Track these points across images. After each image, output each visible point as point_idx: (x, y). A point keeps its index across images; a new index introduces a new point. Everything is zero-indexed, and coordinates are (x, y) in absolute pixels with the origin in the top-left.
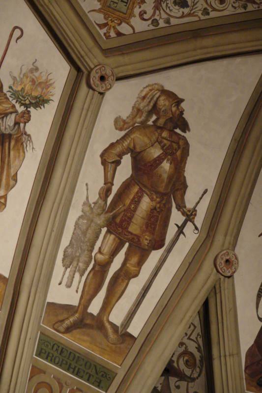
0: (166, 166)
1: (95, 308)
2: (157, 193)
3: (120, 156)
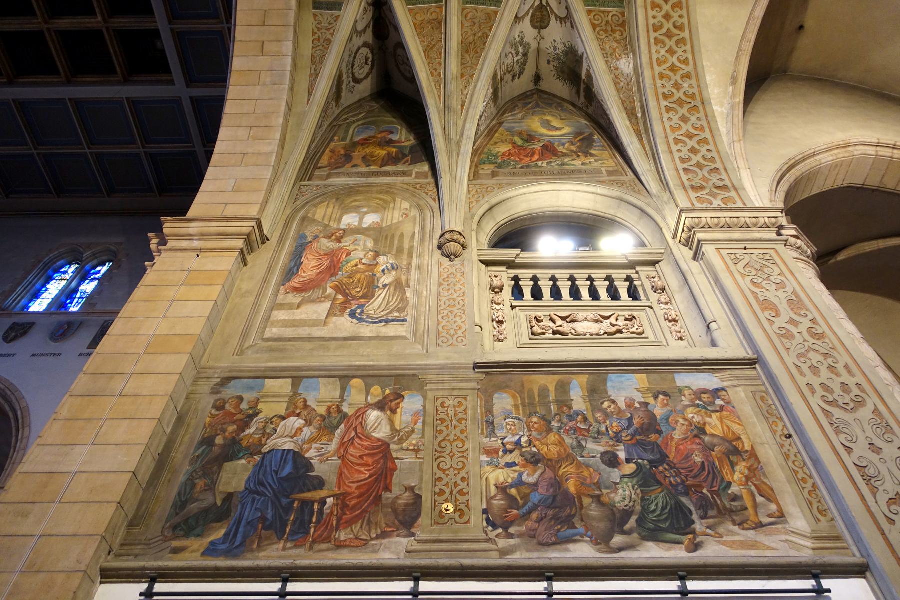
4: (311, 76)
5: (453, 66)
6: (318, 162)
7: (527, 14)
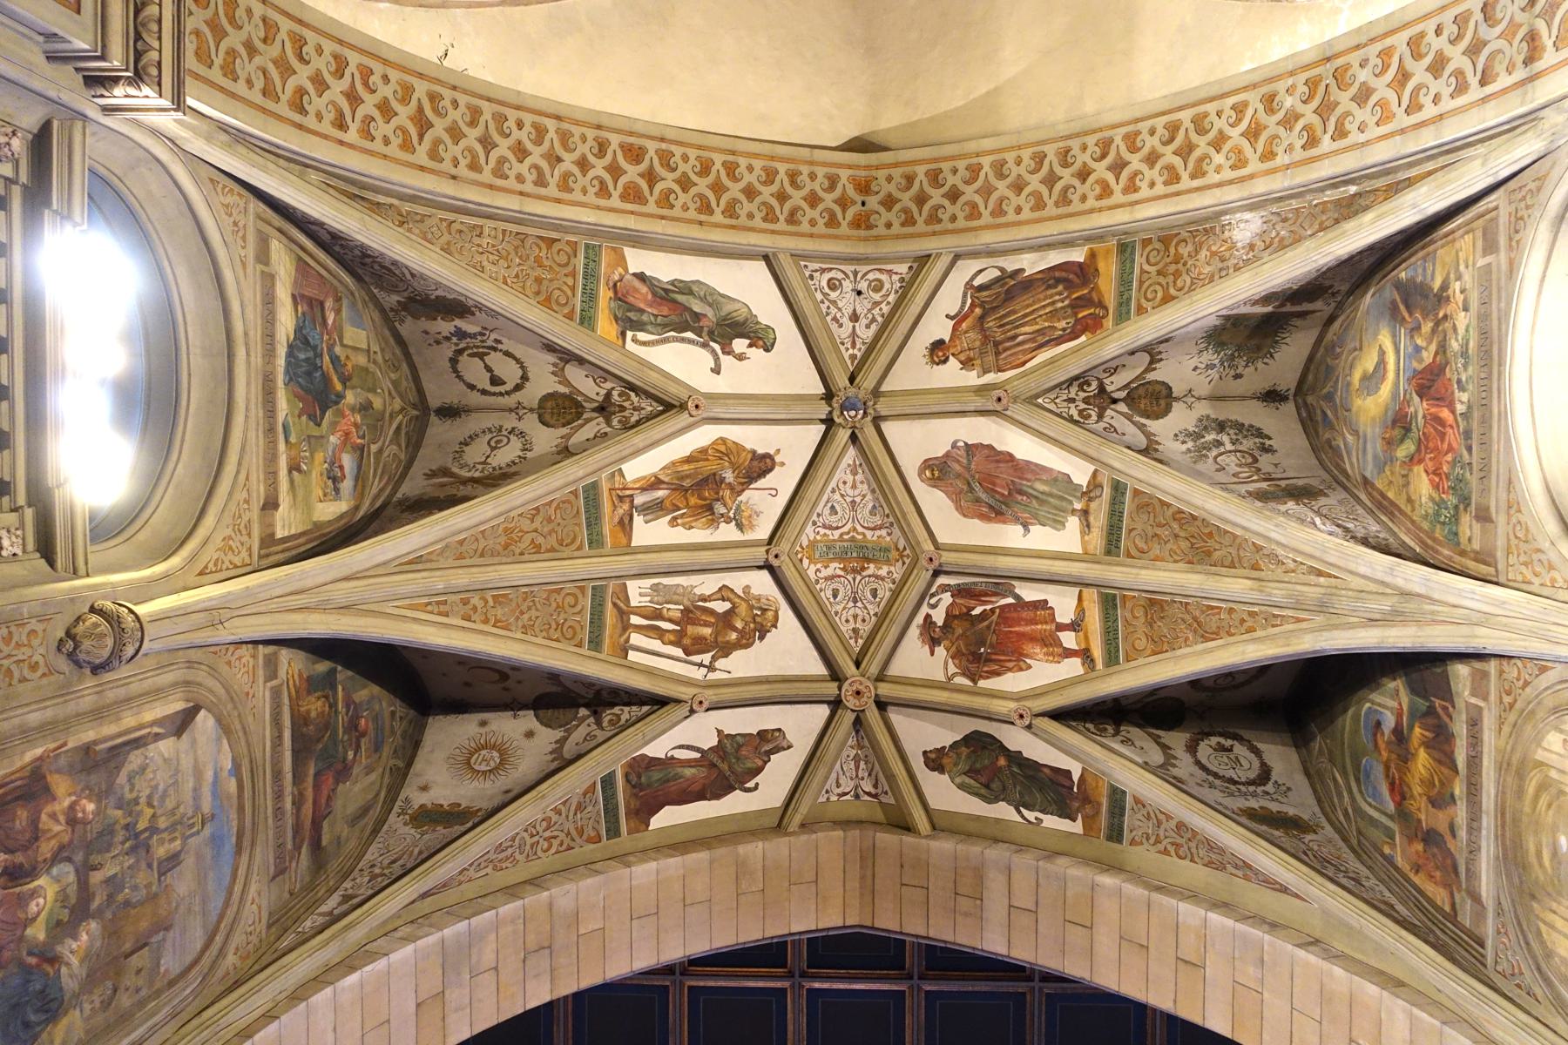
0: (734, 636)
1: (635, 620)
2: (716, 638)
3: (729, 600)
4: (1246, 878)
5: (1234, 586)
6: (1440, 909)
7: (1141, 427)
